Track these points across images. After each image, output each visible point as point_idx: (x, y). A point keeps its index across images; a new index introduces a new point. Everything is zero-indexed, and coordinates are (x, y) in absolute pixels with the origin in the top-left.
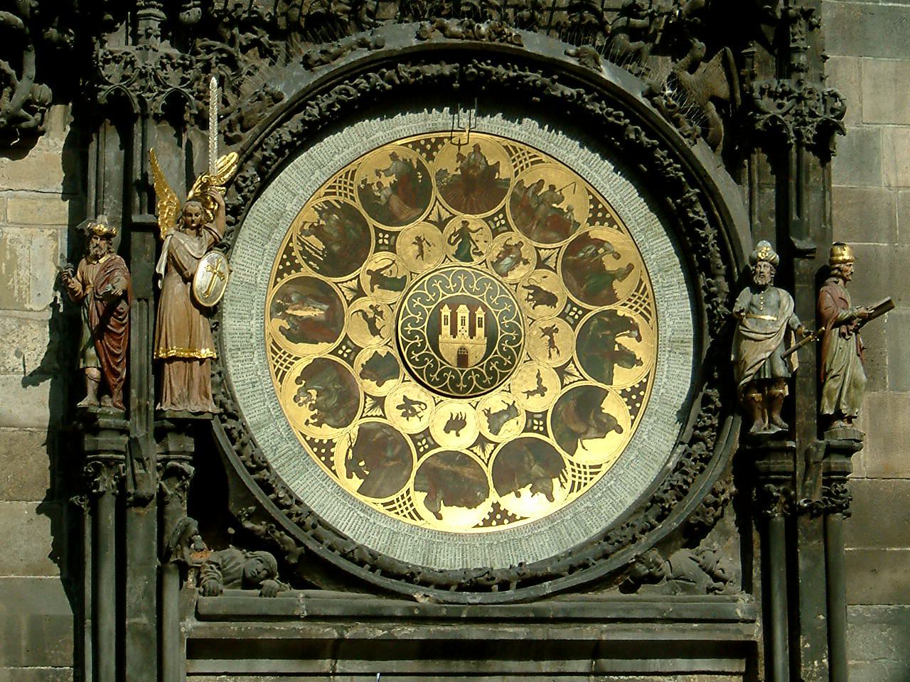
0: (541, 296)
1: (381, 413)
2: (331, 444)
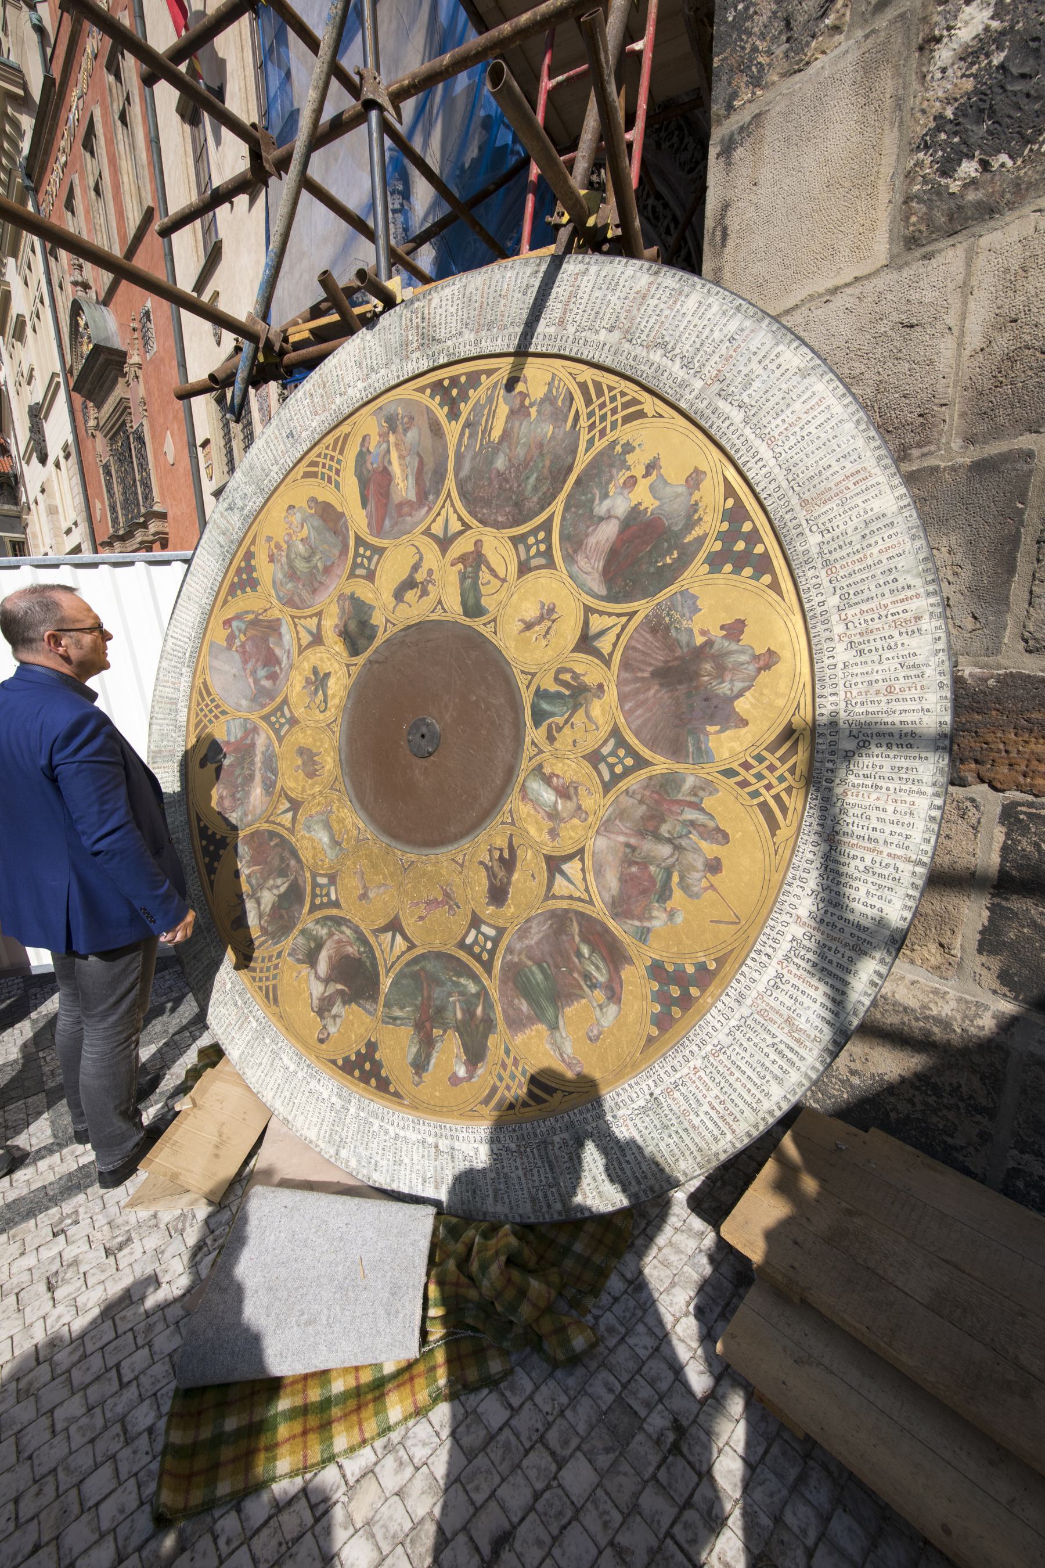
0: (501, 874)
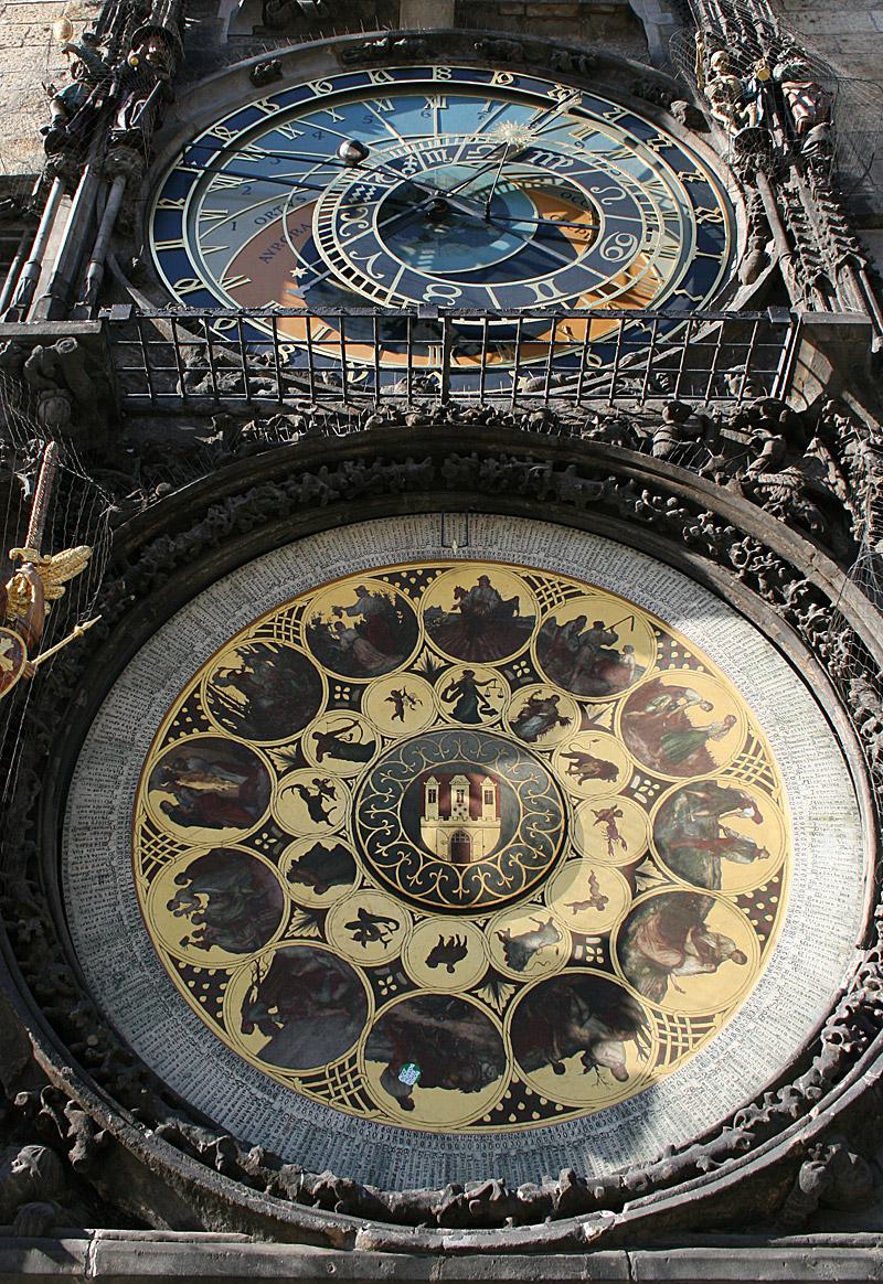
0: (591, 767)
1: (317, 933)
2: (222, 976)
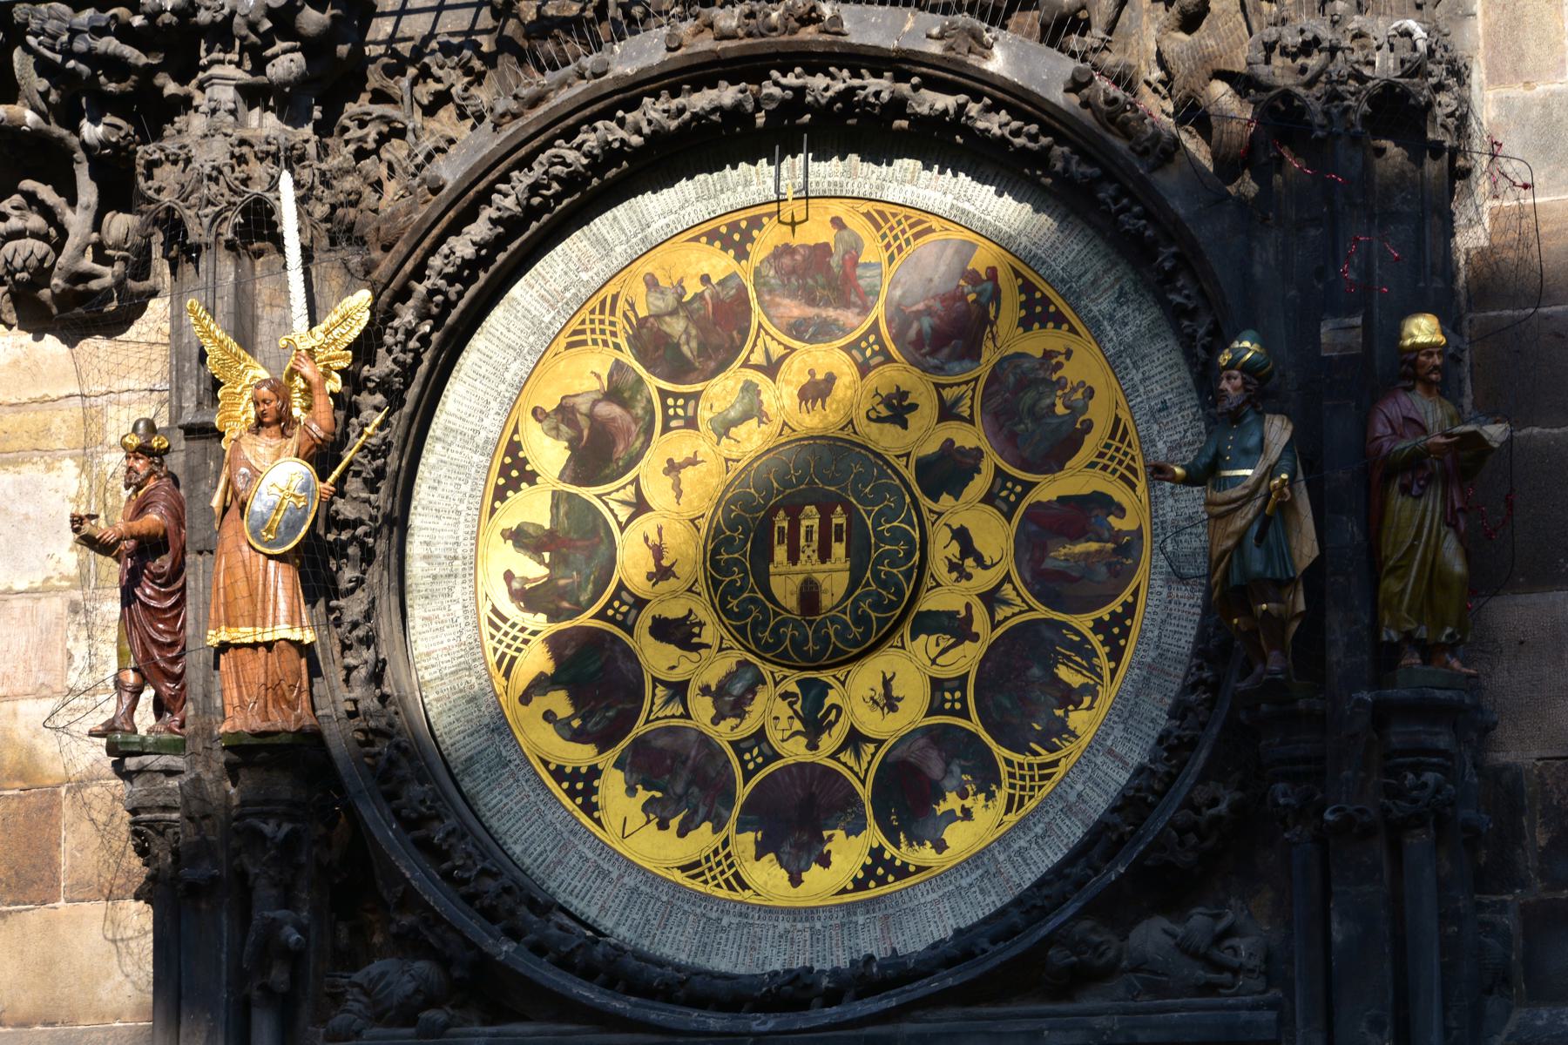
2: (1026, 324)
